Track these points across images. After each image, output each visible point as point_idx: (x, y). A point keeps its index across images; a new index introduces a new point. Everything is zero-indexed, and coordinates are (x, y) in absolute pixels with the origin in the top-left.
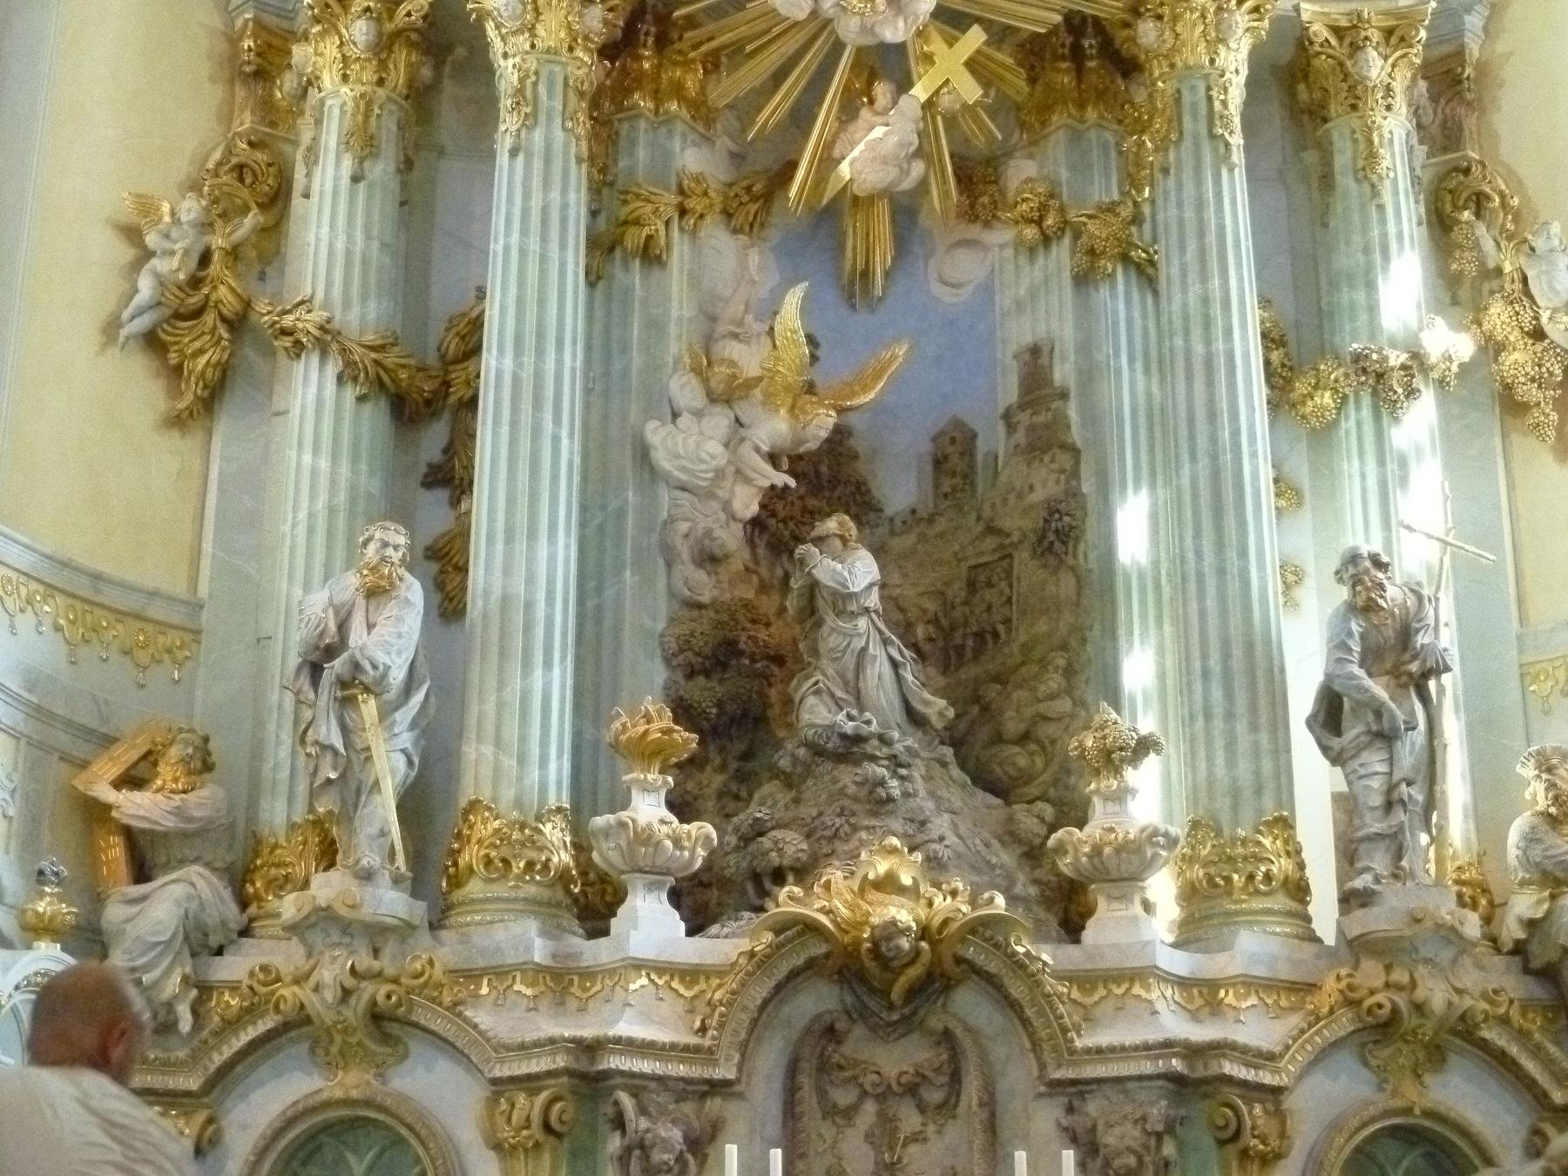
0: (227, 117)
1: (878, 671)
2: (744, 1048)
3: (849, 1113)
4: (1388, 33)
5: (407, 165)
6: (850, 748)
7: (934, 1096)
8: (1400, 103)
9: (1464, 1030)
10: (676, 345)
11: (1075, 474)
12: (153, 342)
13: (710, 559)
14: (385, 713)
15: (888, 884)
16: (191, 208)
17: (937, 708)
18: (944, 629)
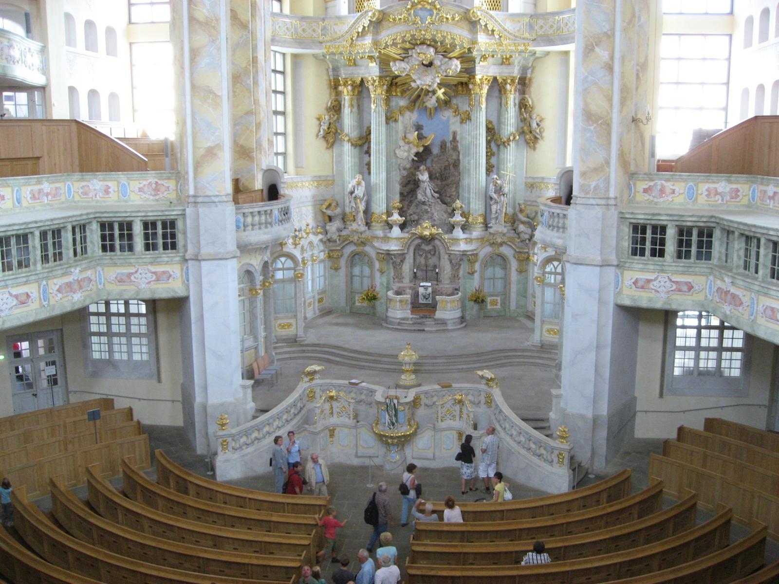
0: (330, 94)
1: (428, 190)
2: (408, 249)
3: (421, 255)
4: (512, 80)
5: (359, 105)
6: (424, 203)
7: (432, 253)
8: (513, 92)
9: (504, 243)
10: (401, 135)
11: (459, 156)
12: (324, 137)
13: (405, 169)
14: (361, 200)
15: (426, 227)
16: (327, 117)
17: (436, 195)
18: (441, 175)
